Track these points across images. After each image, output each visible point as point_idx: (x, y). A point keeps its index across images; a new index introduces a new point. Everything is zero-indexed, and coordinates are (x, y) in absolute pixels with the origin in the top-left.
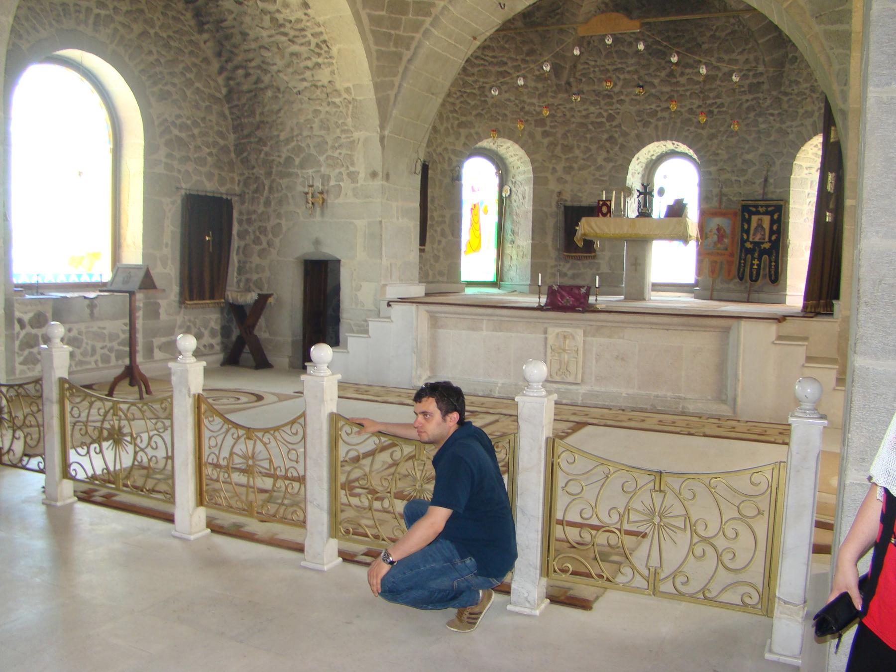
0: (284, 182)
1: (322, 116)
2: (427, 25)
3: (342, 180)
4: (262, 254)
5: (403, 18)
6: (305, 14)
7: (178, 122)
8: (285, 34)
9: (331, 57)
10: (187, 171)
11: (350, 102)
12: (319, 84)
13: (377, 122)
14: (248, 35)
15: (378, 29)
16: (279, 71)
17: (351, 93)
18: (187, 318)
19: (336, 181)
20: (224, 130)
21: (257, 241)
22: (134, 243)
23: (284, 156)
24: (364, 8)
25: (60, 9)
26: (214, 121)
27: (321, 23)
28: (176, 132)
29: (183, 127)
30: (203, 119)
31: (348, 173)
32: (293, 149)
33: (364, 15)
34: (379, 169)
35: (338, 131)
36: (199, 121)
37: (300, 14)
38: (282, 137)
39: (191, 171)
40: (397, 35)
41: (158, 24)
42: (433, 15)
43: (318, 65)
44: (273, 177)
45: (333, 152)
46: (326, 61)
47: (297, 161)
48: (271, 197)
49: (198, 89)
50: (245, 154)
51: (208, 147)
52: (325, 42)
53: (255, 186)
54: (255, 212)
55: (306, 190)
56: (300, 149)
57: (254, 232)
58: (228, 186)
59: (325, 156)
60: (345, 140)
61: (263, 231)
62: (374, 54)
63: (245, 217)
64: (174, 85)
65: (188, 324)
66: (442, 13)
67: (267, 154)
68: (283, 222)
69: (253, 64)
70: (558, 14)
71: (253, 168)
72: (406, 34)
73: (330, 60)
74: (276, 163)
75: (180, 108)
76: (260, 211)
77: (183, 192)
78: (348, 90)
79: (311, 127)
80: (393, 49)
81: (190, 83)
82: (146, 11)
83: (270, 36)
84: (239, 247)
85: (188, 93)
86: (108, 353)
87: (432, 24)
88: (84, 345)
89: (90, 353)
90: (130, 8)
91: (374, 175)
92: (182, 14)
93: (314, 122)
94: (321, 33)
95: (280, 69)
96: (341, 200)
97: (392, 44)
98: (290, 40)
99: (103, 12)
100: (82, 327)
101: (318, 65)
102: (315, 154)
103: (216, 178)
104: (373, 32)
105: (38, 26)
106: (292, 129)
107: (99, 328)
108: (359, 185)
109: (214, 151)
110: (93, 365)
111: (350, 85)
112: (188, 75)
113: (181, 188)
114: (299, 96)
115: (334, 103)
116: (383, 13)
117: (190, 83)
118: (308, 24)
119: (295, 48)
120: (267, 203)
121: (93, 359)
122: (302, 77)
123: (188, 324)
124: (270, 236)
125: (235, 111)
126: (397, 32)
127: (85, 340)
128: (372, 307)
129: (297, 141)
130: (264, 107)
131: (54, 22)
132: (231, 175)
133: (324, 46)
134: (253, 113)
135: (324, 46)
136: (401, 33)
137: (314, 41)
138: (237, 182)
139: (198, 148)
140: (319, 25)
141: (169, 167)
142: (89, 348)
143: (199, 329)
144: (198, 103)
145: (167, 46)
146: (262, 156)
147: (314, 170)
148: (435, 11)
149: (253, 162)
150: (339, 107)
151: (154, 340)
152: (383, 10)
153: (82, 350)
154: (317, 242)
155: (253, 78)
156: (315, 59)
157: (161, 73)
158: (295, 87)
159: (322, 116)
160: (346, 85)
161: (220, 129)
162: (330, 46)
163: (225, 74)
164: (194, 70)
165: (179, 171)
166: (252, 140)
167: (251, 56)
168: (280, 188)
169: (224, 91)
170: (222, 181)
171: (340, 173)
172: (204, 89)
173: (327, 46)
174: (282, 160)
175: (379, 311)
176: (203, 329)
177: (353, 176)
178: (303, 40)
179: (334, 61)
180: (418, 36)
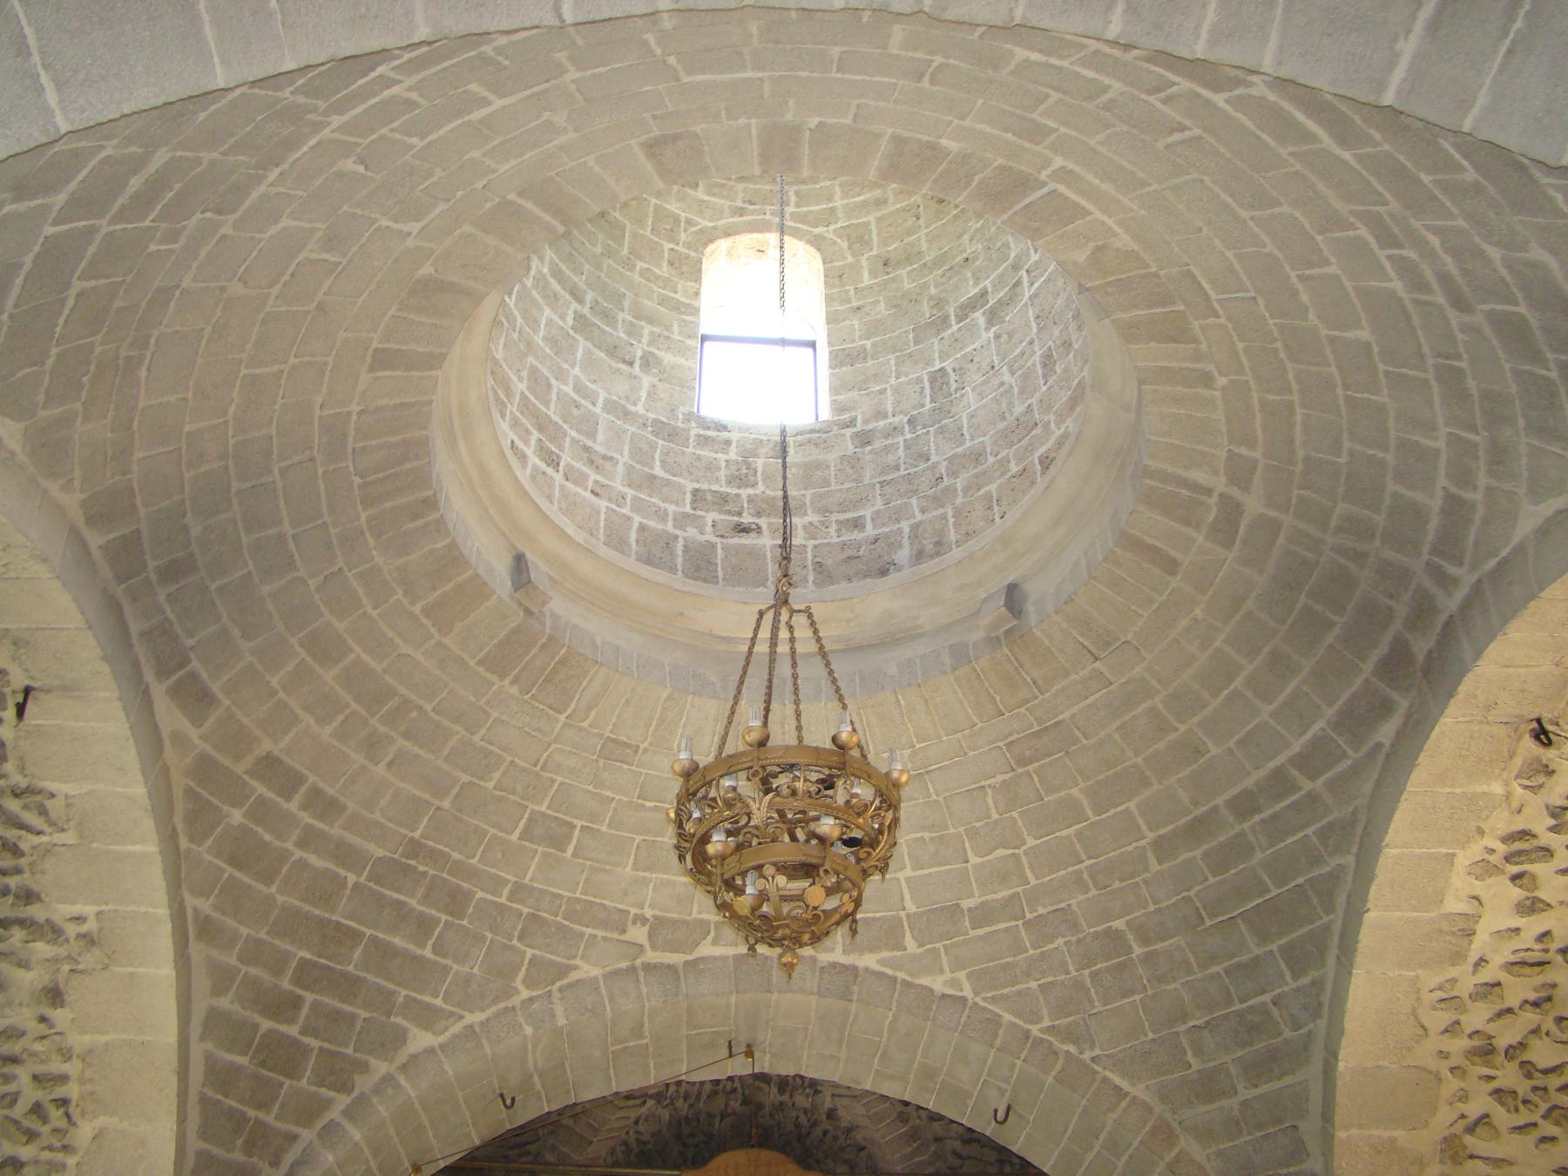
2: (334, 1113)
5: (287, 1082)
6: (43, 1019)
15: (220, 1097)
27: (77, 1050)
33: (198, 1050)
37: (24, 1017)
42: (355, 1094)
52: (63, 1102)
66: (377, 1090)
70: (528, 1153)
72: (278, 1125)
80: (238, 1156)
87: (348, 1113)
94: (63, 1079)
97: (240, 1142)
104: (204, 1100)
116: (242, 1060)
118: (38, 1047)
126: (261, 1115)
135: (55, 1114)
136: (269, 1119)
140: (67, 1055)
148: (363, 1083)
152: (244, 1054)
162: (76, 1117)
173: (67, 1115)
180: (307, 1135)
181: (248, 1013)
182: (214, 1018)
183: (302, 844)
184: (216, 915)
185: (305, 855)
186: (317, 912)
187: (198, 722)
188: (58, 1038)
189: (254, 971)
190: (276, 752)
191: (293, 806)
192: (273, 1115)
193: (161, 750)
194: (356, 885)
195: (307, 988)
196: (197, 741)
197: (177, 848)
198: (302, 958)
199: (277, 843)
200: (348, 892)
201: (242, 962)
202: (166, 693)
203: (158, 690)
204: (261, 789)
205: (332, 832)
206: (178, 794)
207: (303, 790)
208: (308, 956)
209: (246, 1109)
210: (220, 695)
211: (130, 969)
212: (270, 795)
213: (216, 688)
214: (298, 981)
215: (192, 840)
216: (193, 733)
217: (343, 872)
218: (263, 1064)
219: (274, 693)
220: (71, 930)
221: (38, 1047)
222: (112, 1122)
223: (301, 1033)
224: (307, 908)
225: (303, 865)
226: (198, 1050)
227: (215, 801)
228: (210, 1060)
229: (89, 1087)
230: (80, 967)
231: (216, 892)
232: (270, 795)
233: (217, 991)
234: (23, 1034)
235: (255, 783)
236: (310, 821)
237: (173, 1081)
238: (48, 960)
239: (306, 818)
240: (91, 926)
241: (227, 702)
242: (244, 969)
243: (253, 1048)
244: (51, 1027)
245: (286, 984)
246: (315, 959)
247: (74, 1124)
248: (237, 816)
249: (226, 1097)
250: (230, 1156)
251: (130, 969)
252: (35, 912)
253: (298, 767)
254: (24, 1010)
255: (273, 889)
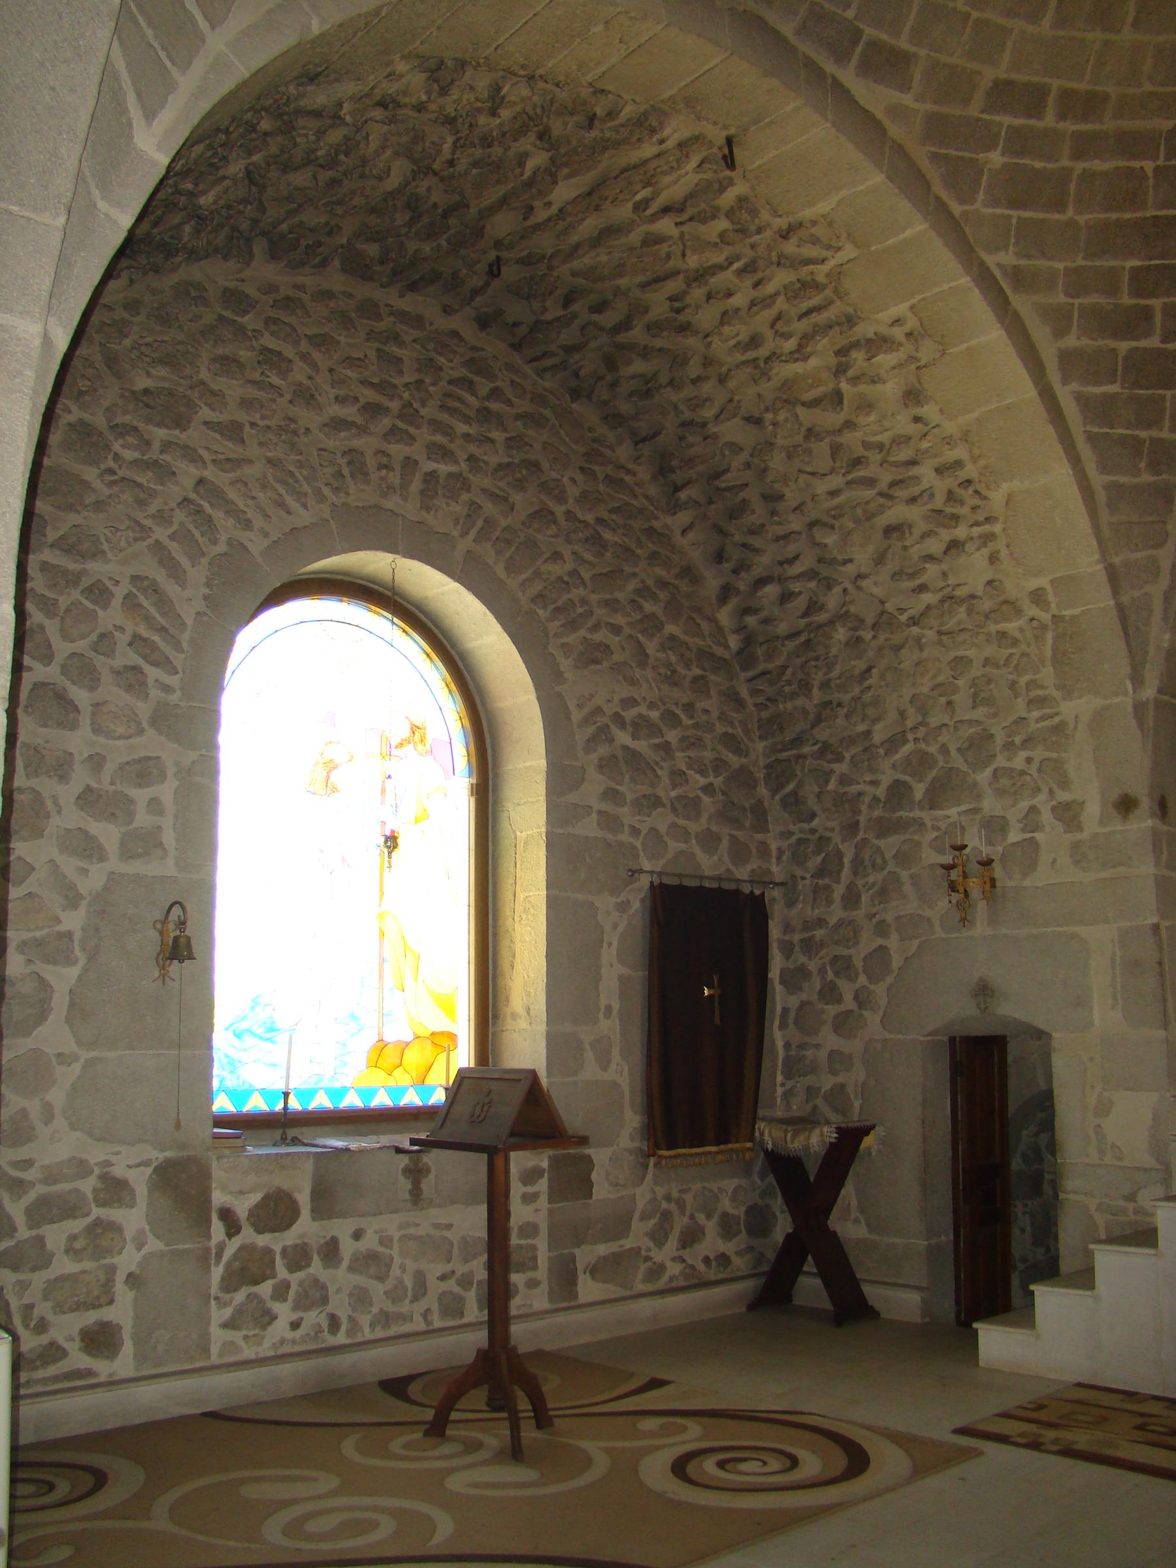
0: (890, 844)
1: (976, 671)
3: (1037, 827)
4: (844, 1024)
6: (917, 419)
7: (630, 714)
8: (870, 482)
9: (988, 520)
10: (653, 830)
11: (1043, 627)
12: (961, 592)
13: (1126, 670)
14: (780, 497)
16: (859, 576)
17: (1047, 604)
18: (660, 1191)
19: (1023, 830)
20: (739, 731)
21: (830, 993)
22: (528, 1010)
23: (886, 780)
24: (1065, 381)
25: (343, 462)
26: (715, 714)
28: (623, 738)
29: (640, 727)
30: (689, 708)
31: (1054, 809)
32: (908, 759)
34: (1141, 790)
35: (1020, 704)
36: (678, 712)
37: (902, 424)
38: (877, 738)
39: (663, 828)
40: (1155, 442)
41: (573, 492)
43: (954, 546)
44: (860, 836)
45: (1009, 759)
46: (976, 531)
47: (919, 790)
48: (860, 883)
49: (672, 638)
50: (790, 787)
51: (703, 772)
53: (819, 859)
54: (821, 922)
55: (947, 859)
56: (922, 762)
57: (822, 971)
58: (753, 865)
59: (988, 771)
60: (1039, 725)
61: (844, 967)
62: (1101, 497)
63: (797, 937)
64: (616, 629)
65: (664, 1205)
67: (844, 780)
68: (892, 942)
69: (797, 569)
71: (813, 816)
73: (986, 528)
74: (867, 800)
75: (632, 682)
76: (833, 920)
77: (645, 881)
78: (1038, 597)
79: (949, 703)
80: (1147, 478)
81: (651, 624)
82: (545, 464)
83: (833, 494)
84: (785, 1011)
85: (651, 647)
86: (457, 1289)
88: (395, 1271)
89: (410, 1293)
90: (506, 460)
91: (1126, 805)
92: (629, 472)
93: (956, 690)
94: (958, 464)
95: (863, 570)
96: (1042, 876)
97: (1142, 465)
98: (881, 494)
99: (444, 468)
100: (391, 1224)
101: (954, 546)
102: (964, 767)
103: (725, 843)
104: (1091, 438)
105: (290, 500)
106: (902, 714)
107: (437, 1226)
108: (1084, 835)
109: (718, 781)
110: (419, 1325)
111: (1043, 582)
112: (649, 607)
113: (641, 871)
114: (915, 630)
115: (1002, 634)
117: (651, 624)
118: (925, 445)
119: (897, 513)
120: (851, 899)
121: (420, 1306)
122: (918, 582)
123: (664, 1205)
124: (862, 980)
125: (761, 685)
126: (1154, 433)
127: (397, 1261)
128: (1149, 1161)
129: (916, 740)
130: (830, 667)
131: (326, 491)
132: (759, 837)
133: (967, 494)
134: (805, 687)
137: (941, 486)
138: (774, 853)
139: (678, 777)
140: (949, 441)
141: (610, 822)
142: (409, 1282)
143: (692, 1217)
144: (674, 672)
145: (596, 541)
146: (831, 786)
147: (963, 808)
149: (812, 803)
150: (1015, 642)
151: (577, 1252)
153: (390, 1283)
154: (984, 991)
155: (801, 603)
156: (946, 535)
157: (584, 601)
158: (901, 610)
159: (976, 671)
160: (1033, 584)
161: (730, 730)
162: (985, 492)
163: (733, 603)
164: (663, 595)
165: (635, 831)
166: (806, 750)
167: (792, 549)
168: (879, 861)
169: (734, 642)
170: (739, 853)
171: (1033, 809)
172: (686, 639)
173: (977, 492)
174: (881, 792)
175: (1168, 1169)
176: (701, 1218)
177: (1068, 814)
178: (916, 490)
179: (997, 528)
181: (1100, 343)
182: (1067, 359)
183: (1078, 155)
184: (1023, 262)
185: (1087, 165)
186: (1127, 216)
187: (905, 87)
188: (934, 431)
189: (1086, 301)
190: (1003, 76)
191: (1049, 120)
192: (1166, 429)
193: (883, 131)
194: (1157, 169)
195: (1149, 296)
196: (915, 106)
197: (951, 215)
198: (1132, 268)
199: (1050, 166)
200: (1151, 181)
201: (1072, 297)
202: (857, 75)
203: (848, 76)
204: (1007, 120)
205: (1105, 127)
206: (925, 165)
207: (1051, 101)
208: (1137, 263)
209: (1137, 432)
210: (912, 49)
211: (965, 346)
212: (1019, 122)
213: (903, 43)
214: (1137, 293)
215: (962, 201)
216: (907, 99)
217: (1136, 164)
218: (1136, 385)
219: (967, 16)
220: (898, 333)
221: (925, 445)
222: (1015, 485)
223: (1163, 341)
224: (1114, 216)
225: (1088, 176)
226: (1065, 395)
227: (967, 155)
228: (1079, 397)
229: (982, 462)
230: (923, 362)
231: (1013, 241)
232: (1019, 122)
233: (1060, 332)
234: (910, 438)
235: (997, 118)
236: (1077, 127)
237: (1050, 430)
238: (894, 368)
239: (1070, 126)
240: (912, 323)
241: (923, 52)
242: (1077, 302)
243: (1119, 373)
244: (926, 424)
245: (1127, 300)
246: (1146, 263)
247: (985, 498)
248: (996, 158)
249: (1112, 427)
250: (1137, 480)
251: (965, 346)
252: (864, 330)
253: (1035, 79)
254: (899, 418)
255: (1070, 213)
